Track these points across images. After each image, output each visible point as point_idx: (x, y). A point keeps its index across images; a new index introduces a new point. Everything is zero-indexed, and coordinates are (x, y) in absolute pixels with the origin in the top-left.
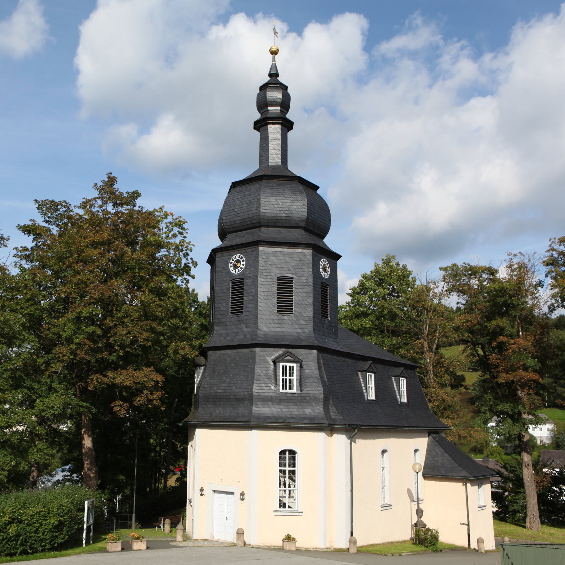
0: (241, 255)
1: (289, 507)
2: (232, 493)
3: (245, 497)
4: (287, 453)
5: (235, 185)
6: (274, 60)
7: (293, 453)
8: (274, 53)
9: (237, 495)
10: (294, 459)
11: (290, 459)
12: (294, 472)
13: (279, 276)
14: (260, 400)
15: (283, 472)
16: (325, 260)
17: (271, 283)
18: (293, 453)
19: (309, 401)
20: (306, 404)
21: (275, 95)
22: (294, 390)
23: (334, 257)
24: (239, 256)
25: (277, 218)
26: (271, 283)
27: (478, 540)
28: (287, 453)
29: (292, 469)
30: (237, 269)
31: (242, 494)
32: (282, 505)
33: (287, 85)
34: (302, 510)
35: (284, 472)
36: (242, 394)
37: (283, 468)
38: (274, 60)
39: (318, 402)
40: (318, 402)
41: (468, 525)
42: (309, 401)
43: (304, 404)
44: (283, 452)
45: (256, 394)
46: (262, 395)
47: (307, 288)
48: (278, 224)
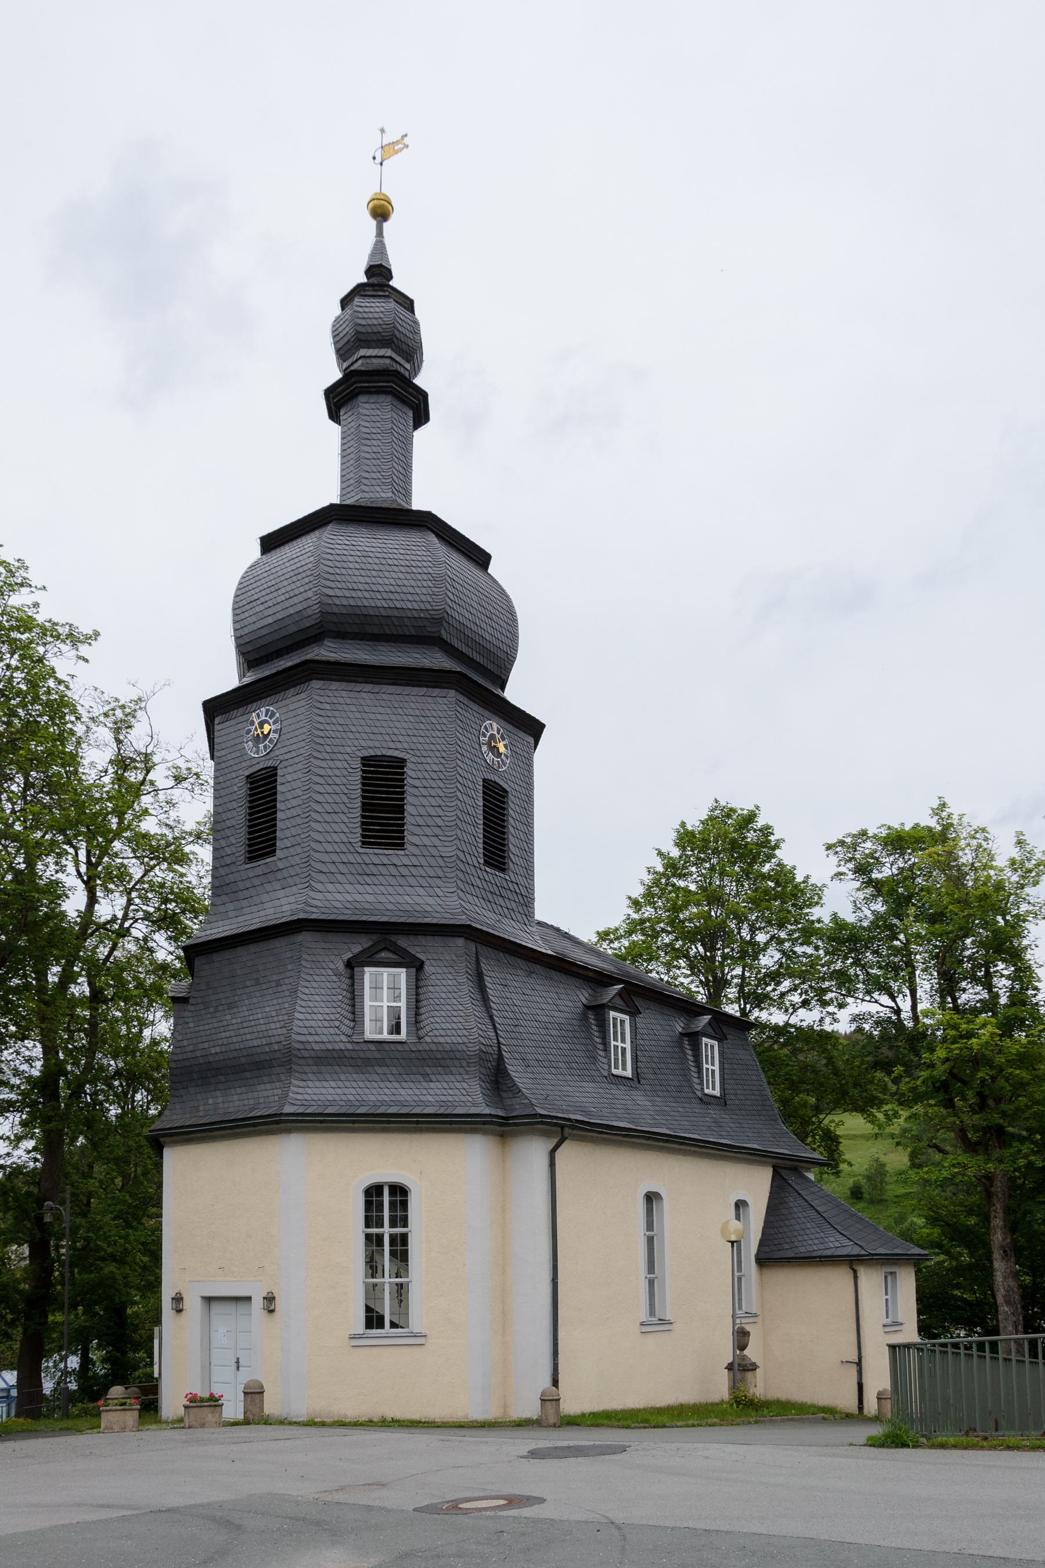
0: (271, 708)
1: (393, 1325)
2: (248, 1299)
3: (279, 1304)
4: (386, 1191)
5: (271, 543)
6: (380, 233)
7: (400, 1192)
8: (381, 213)
9: (258, 1303)
10: (404, 1205)
11: (392, 1204)
12: (404, 1238)
13: (366, 753)
14: (311, 1061)
15: (373, 1241)
16: (495, 725)
17: (345, 772)
18: (400, 1192)
19: (442, 1062)
20: (434, 1069)
21: (376, 309)
22: (403, 1036)
23: (533, 728)
24: (267, 711)
25: (365, 612)
26: (345, 772)
27: (879, 1394)
28: (386, 1191)
29: (399, 1230)
30: (261, 746)
31: (270, 1299)
32: (373, 1320)
33: (411, 297)
34: (424, 1331)
35: (380, 1239)
36: (267, 1049)
37: (374, 1230)
38: (380, 233)
39: (464, 1063)
40: (464, 1063)
41: (859, 1364)
42: (442, 1062)
43: (428, 1070)
44: (373, 1193)
45: (300, 1046)
46: (316, 1047)
47: (442, 785)
48: (369, 630)
